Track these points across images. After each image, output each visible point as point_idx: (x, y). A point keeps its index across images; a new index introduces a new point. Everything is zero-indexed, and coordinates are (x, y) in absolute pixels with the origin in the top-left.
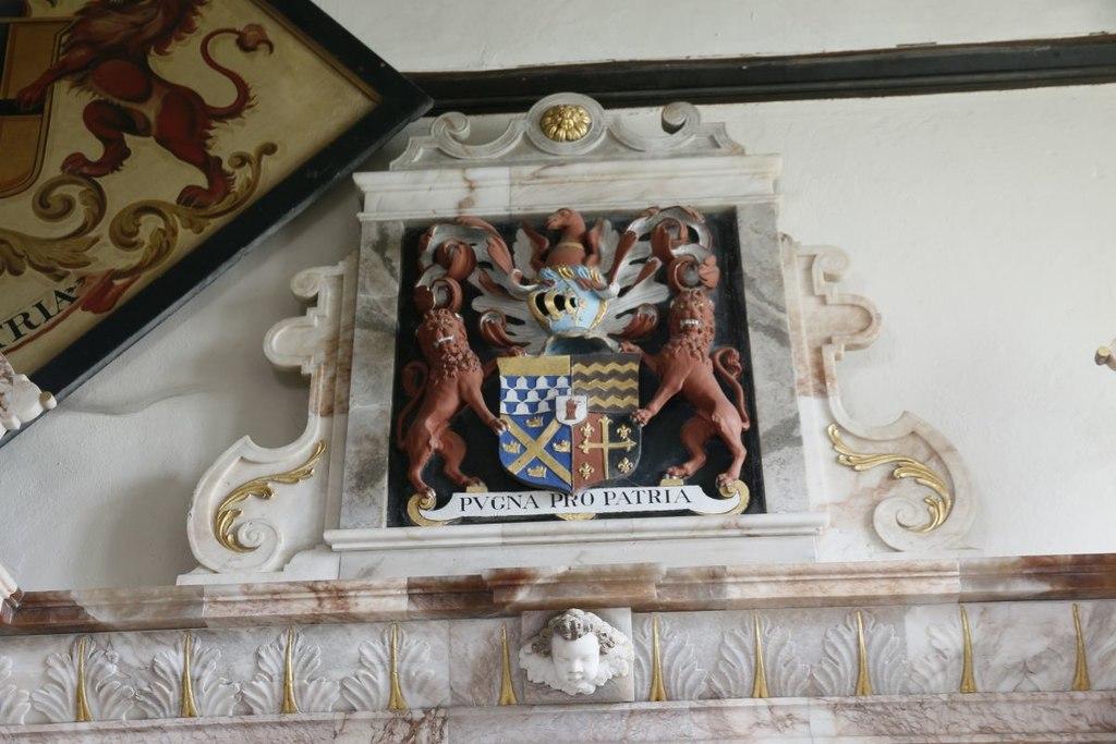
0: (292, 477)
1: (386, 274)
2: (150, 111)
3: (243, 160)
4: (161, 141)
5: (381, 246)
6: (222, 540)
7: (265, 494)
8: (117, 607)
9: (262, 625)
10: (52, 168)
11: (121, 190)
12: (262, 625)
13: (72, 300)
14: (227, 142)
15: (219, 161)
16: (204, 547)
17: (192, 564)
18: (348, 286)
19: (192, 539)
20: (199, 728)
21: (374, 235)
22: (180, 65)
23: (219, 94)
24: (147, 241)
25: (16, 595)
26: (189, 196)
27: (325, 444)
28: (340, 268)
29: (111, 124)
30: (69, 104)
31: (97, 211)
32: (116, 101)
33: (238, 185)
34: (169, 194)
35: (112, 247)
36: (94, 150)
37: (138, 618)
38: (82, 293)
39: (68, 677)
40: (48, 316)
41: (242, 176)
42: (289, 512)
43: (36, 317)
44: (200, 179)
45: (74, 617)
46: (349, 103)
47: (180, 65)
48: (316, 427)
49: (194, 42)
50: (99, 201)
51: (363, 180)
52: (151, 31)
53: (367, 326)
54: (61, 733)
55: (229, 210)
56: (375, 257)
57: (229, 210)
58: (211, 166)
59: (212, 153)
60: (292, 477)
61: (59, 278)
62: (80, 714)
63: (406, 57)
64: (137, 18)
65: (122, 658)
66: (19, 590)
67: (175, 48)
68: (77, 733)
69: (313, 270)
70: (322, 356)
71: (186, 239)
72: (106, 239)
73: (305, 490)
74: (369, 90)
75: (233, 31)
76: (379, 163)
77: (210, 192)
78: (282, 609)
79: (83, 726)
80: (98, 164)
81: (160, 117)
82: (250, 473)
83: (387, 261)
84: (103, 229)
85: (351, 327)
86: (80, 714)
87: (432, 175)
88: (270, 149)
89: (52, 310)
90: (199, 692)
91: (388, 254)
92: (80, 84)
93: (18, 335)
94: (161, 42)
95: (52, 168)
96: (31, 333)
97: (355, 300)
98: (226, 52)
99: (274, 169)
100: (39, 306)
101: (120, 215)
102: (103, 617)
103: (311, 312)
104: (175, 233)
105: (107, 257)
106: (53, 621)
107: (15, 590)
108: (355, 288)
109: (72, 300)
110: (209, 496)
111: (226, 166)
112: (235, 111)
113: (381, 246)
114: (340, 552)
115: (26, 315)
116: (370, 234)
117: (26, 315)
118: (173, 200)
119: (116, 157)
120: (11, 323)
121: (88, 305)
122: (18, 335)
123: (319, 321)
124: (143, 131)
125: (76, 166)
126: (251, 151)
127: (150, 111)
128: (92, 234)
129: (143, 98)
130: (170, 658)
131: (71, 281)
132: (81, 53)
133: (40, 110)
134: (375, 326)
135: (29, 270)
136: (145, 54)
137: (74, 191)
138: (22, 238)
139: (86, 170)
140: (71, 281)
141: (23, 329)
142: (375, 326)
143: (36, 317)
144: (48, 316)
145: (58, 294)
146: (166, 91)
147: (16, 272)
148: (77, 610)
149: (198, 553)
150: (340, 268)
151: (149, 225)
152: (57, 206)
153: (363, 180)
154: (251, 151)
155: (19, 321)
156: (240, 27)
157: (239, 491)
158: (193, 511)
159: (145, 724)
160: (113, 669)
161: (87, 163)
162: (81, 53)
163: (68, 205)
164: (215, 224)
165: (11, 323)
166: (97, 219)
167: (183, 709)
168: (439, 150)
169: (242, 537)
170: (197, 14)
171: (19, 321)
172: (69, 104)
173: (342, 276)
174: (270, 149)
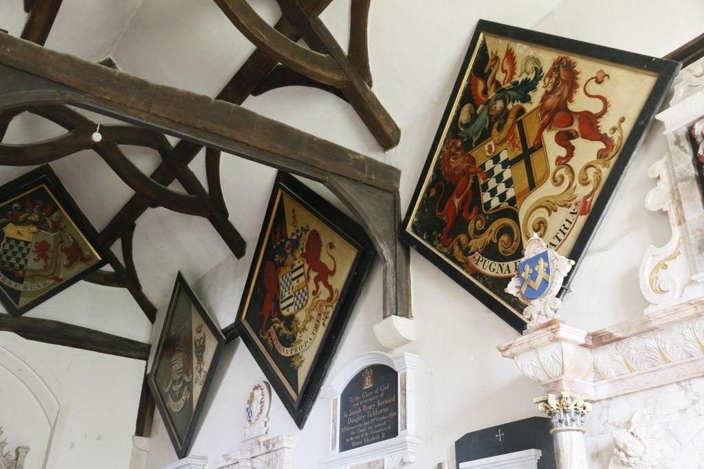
0: (673, 257)
1: (683, 153)
2: (575, 127)
3: (614, 129)
4: (584, 137)
5: (677, 142)
6: (655, 291)
7: (665, 267)
8: (623, 330)
9: (679, 322)
10: (553, 167)
11: (577, 163)
12: (679, 322)
13: (575, 213)
14: (605, 126)
15: (606, 134)
16: (650, 296)
17: (648, 304)
18: (670, 165)
19: (644, 294)
20: (676, 365)
21: (674, 139)
22: (579, 103)
23: (595, 107)
24: (593, 179)
25: (589, 335)
26: (601, 155)
27: (682, 237)
28: (665, 158)
29: (565, 139)
30: (549, 137)
31: (572, 175)
32: (563, 129)
33: (616, 142)
34: (593, 157)
35: (582, 187)
36: (563, 152)
37: (631, 332)
38: (578, 209)
39: (621, 358)
40: (571, 223)
41: (616, 137)
42: (677, 272)
43: (567, 225)
44: (601, 145)
45: (610, 337)
46: (645, 83)
47: (579, 103)
48: (676, 231)
49: (580, 90)
50: (572, 171)
51: (659, 117)
52: (565, 95)
53: (682, 180)
54: (628, 377)
55: (617, 152)
56: (676, 148)
57: (617, 152)
58: (604, 138)
59: (602, 132)
60: (673, 257)
61: (569, 207)
62: (632, 370)
63: (660, 50)
64: (559, 93)
65: (635, 345)
66: (588, 333)
67: (575, 97)
68: (633, 376)
69: (655, 164)
70: (670, 200)
71: (605, 172)
72: (579, 185)
73: (681, 259)
74: (652, 73)
75: (592, 78)
76: (665, 106)
77: (607, 149)
78: (682, 315)
79: (634, 374)
80: (567, 157)
81: (580, 127)
82: (657, 260)
83: (682, 147)
84: (576, 182)
85: (676, 184)
86: (632, 370)
87: (688, 100)
88: (622, 120)
89: (571, 221)
90: (668, 353)
91: (682, 144)
92: (550, 129)
93: (564, 234)
94: (570, 98)
95: (553, 167)
96: (568, 231)
97: (674, 172)
98: (594, 88)
99: (627, 128)
100: (567, 220)
101: (580, 174)
102: (619, 335)
103: (659, 183)
104: (601, 172)
105: (582, 192)
106: (604, 341)
107: (586, 334)
108: (673, 166)
109: (575, 213)
110: (645, 275)
111: (609, 135)
112: (604, 111)
113: (677, 142)
114: (702, 282)
115: (564, 225)
116: (672, 139)
117: (564, 225)
118: (595, 158)
119: (571, 150)
120: (560, 230)
121: (583, 213)
122: (564, 234)
123: (664, 186)
125: (562, 162)
127: (575, 127)
128: (573, 186)
129: (571, 124)
130: (650, 342)
131: (573, 207)
132: (546, 117)
133: (541, 146)
134: (686, 179)
135: (559, 208)
136: (566, 105)
137: (562, 171)
138: (552, 197)
139: (563, 161)
140: (573, 207)
141: (565, 231)
142: (686, 179)
143: (567, 225)
144: (571, 223)
145: (571, 213)
146: (579, 116)
147: (556, 211)
148: (611, 335)
149: (648, 299)
150: (665, 158)
152: (559, 180)
153: (659, 117)
154: (615, 124)
155: (563, 228)
156: (595, 75)
157: (655, 270)
158: (641, 283)
159: (654, 368)
161: (563, 158)
162: (546, 117)
163: (562, 177)
164: (613, 161)
165: (560, 230)
166: (573, 179)
167: (666, 361)
168: (689, 86)
169: (663, 288)
170: (577, 79)
171: (563, 228)
172: (549, 137)
173: (667, 162)
174: (622, 120)
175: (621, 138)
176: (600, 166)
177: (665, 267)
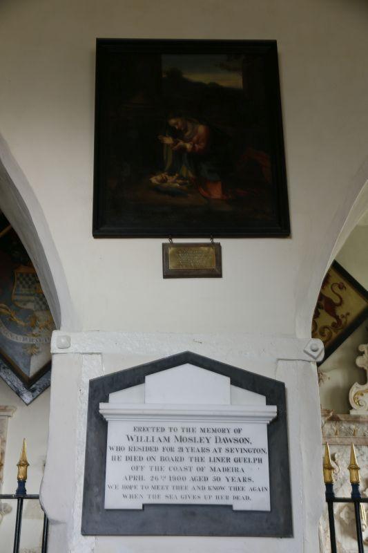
3: (343, 317)
4: (327, 311)
7: (362, 395)
14: (340, 312)
16: (353, 405)
17: (351, 408)
23: (336, 300)
26: (334, 325)
34: (330, 325)
39: (335, 428)
41: (343, 321)
44: (335, 321)
49: (330, 286)
58: (337, 317)
65: (345, 426)
71: (334, 335)
72: (318, 334)
75: (336, 283)
86: (336, 434)
88: (348, 314)
98: (337, 289)
99: (350, 319)
110: (352, 394)
111: (340, 318)
124: (322, 308)
126: (344, 314)
130: (353, 427)
151: (327, 332)
154: (344, 314)
156: (338, 283)
160: (343, 427)
167: (354, 435)
174: (348, 314)
175: (346, 323)
176: (332, 331)
177: (362, 395)
